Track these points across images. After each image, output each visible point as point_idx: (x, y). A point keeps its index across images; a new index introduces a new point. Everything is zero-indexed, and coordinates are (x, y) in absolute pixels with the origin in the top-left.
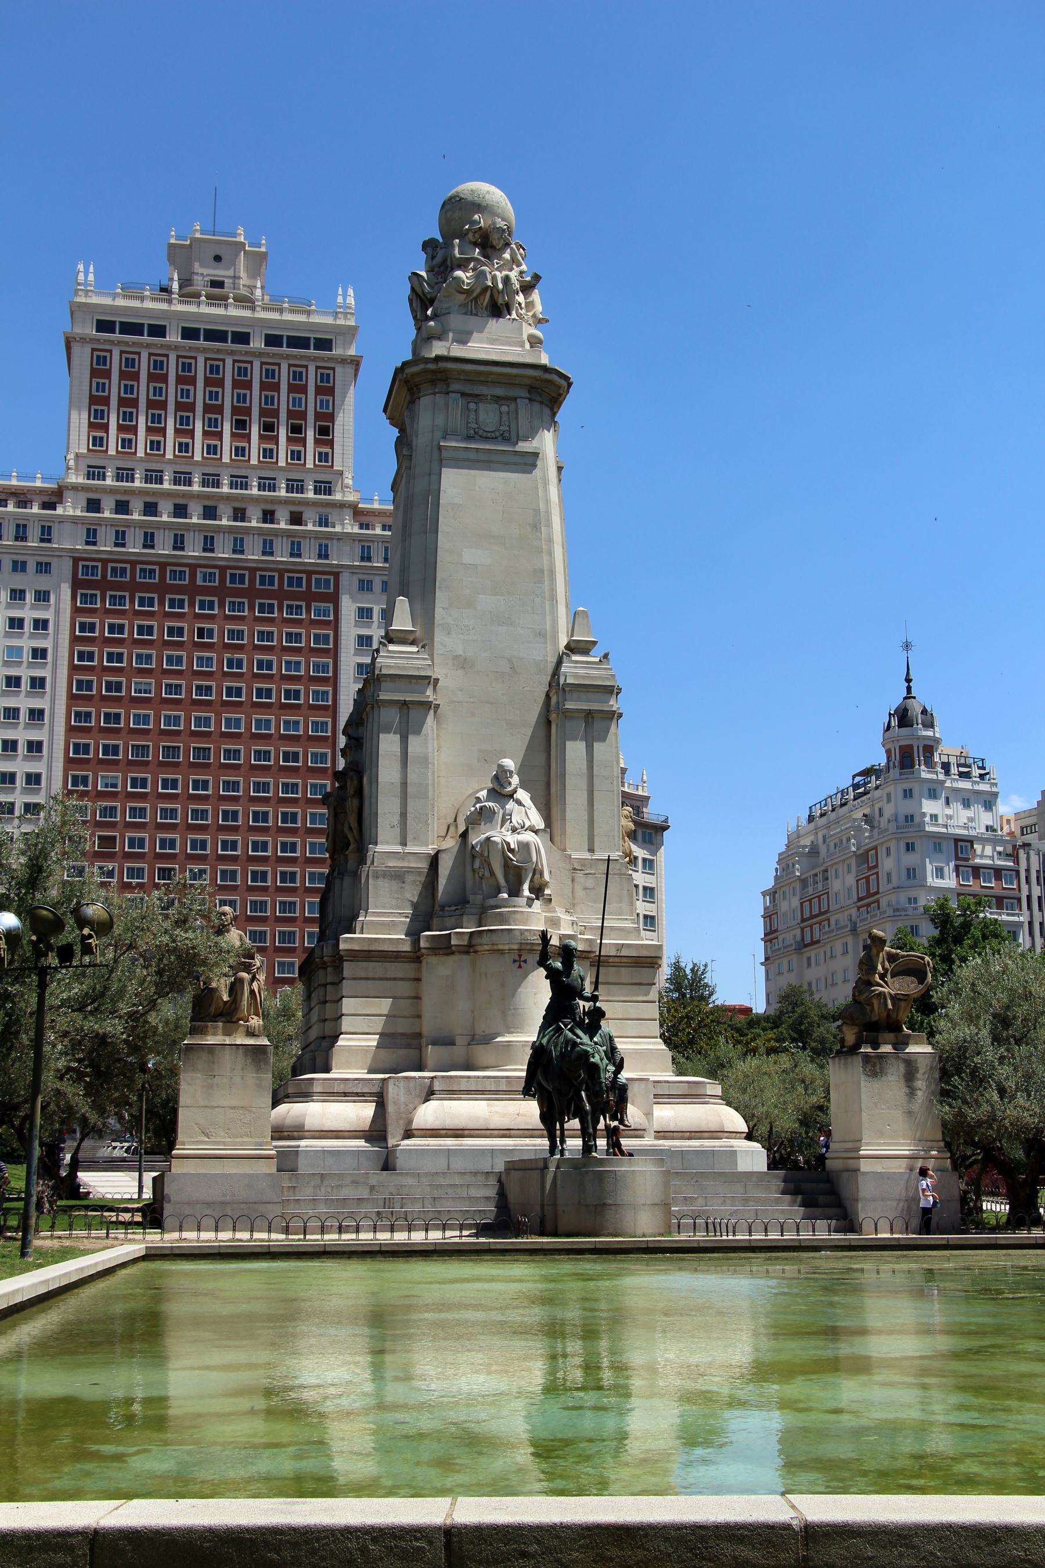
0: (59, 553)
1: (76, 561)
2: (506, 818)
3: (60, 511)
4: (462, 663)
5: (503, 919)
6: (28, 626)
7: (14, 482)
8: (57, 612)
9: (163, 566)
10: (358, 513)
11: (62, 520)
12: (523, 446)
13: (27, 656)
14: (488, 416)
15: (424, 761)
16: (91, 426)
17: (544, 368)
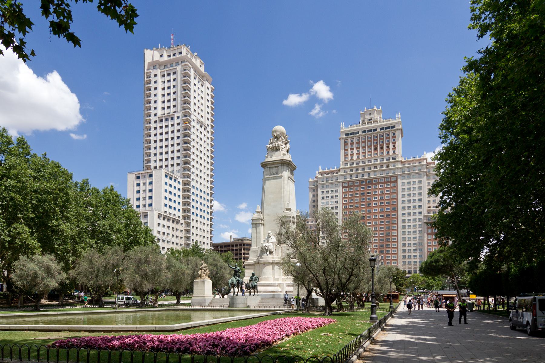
0: (339, 182)
1: (343, 183)
2: (268, 241)
3: (339, 174)
4: (268, 215)
5: (266, 258)
6: (334, 197)
7: (331, 170)
8: (340, 194)
9: (360, 181)
10: (401, 162)
11: (340, 175)
12: (280, 174)
13: (334, 203)
14: (274, 170)
15: (259, 233)
16: (345, 155)
17: (283, 160)
